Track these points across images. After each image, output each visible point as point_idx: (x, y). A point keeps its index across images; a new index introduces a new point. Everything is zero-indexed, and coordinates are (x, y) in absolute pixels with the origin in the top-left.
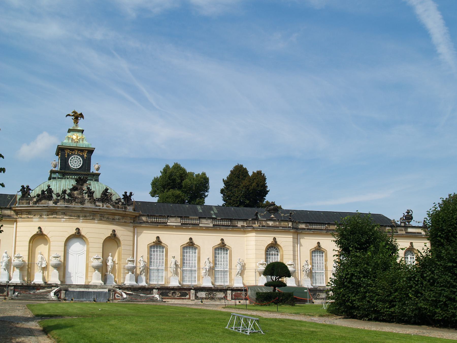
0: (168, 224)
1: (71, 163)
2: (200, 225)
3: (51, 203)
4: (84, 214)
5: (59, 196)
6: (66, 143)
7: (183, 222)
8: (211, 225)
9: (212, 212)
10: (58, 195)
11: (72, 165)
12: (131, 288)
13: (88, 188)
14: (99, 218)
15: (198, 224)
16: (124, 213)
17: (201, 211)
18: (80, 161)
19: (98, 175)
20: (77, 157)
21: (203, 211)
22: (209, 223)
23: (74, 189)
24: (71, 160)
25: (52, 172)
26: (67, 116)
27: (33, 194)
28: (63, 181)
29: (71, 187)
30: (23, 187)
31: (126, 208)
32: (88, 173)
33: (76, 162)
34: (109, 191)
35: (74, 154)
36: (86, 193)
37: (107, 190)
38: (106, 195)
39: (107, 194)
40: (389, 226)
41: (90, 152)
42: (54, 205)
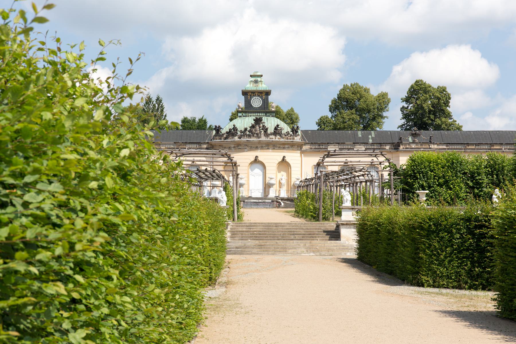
0: (328, 149)
1: (253, 103)
2: (355, 149)
3: (236, 138)
5: (242, 132)
6: (248, 88)
8: (364, 149)
9: (370, 137)
10: (241, 132)
11: (254, 105)
12: (288, 199)
13: (263, 126)
16: (292, 143)
17: (360, 136)
18: (260, 101)
20: (258, 98)
21: (362, 136)
22: (362, 148)
23: (253, 127)
24: (253, 101)
27: (223, 131)
28: (247, 118)
29: (251, 125)
31: (293, 139)
33: (257, 102)
34: (279, 127)
36: (262, 129)
37: (278, 126)
39: (279, 128)
41: (268, 93)
42: (239, 140)
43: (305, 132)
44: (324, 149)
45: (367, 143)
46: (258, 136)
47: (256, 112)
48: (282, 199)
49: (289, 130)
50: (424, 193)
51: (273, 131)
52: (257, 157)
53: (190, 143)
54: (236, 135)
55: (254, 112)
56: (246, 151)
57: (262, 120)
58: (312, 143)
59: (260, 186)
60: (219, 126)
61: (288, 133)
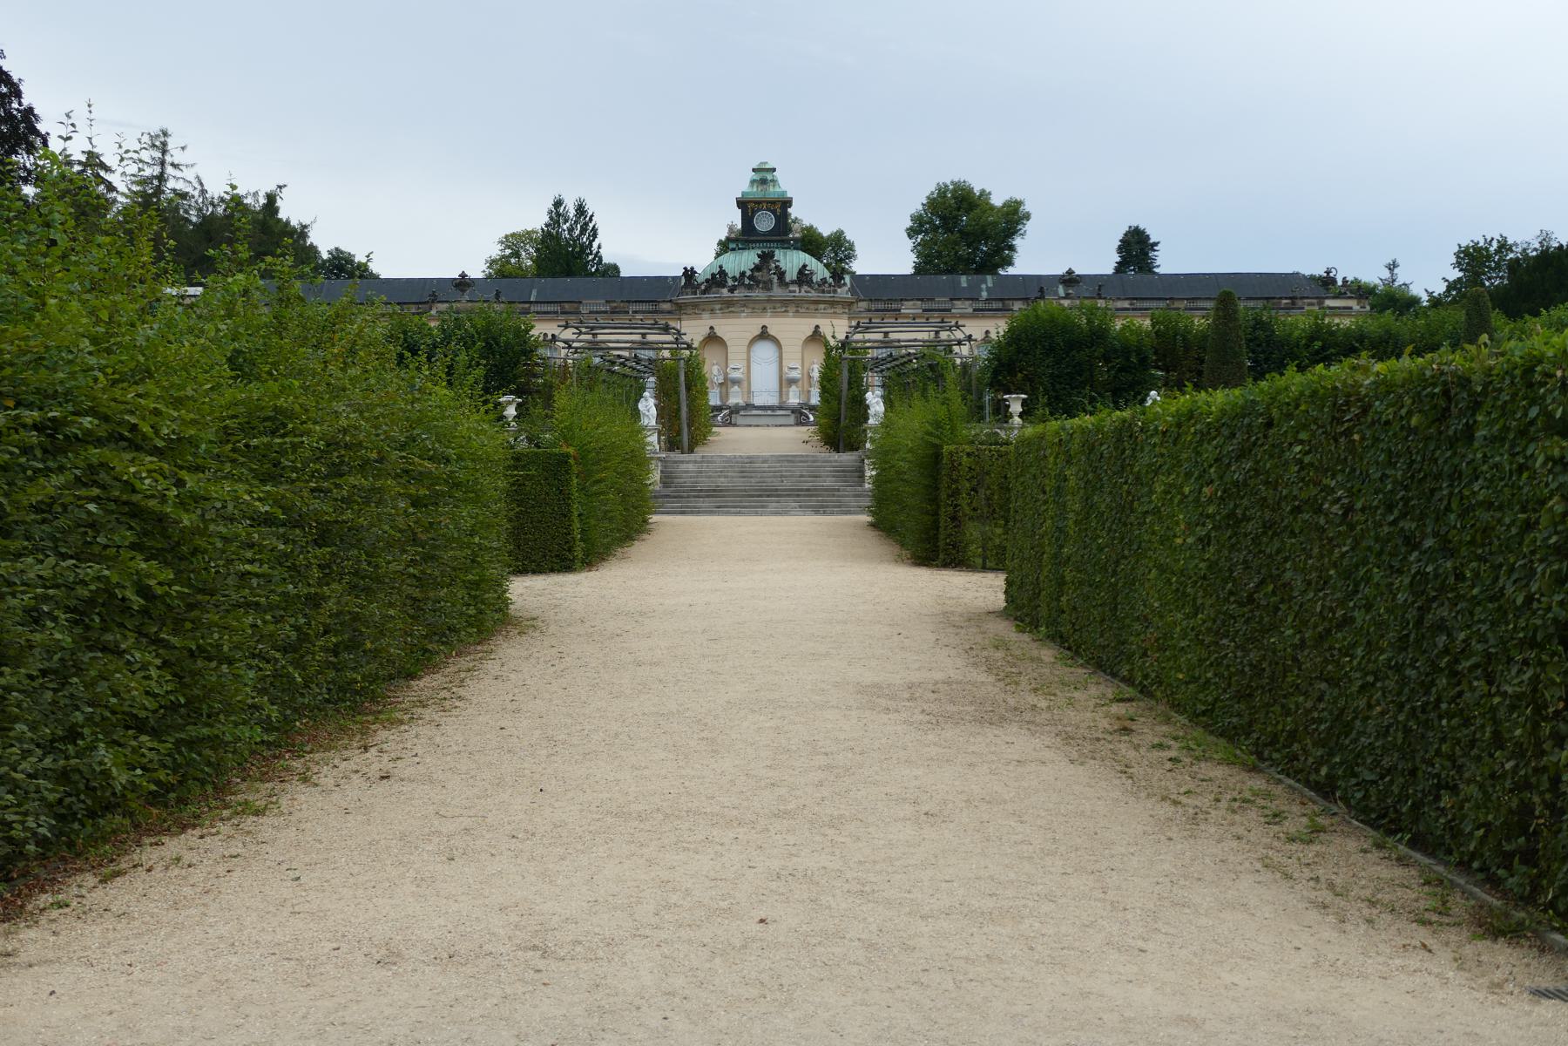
2: (953, 311)
3: (725, 291)
4: (771, 305)
7: (925, 306)
8: (970, 310)
9: (984, 286)
10: (734, 279)
13: (777, 267)
14: (795, 309)
15: (950, 310)
17: (964, 284)
21: (969, 284)
23: (757, 268)
27: (700, 278)
28: (746, 253)
29: (753, 266)
30: (685, 268)
31: (835, 292)
32: (784, 238)
35: (762, 209)
37: (805, 266)
40: (1286, 298)
41: (787, 203)
43: (859, 280)
44: (895, 310)
45: (977, 299)
46: (767, 286)
47: (763, 241)
49: (827, 274)
50: (1018, 398)
51: (795, 278)
52: (764, 327)
53: (636, 302)
54: (724, 286)
55: (759, 241)
56: (745, 317)
57: (773, 256)
58: (871, 300)
59: (773, 384)
60: (692, 268)
61: (824, 281)
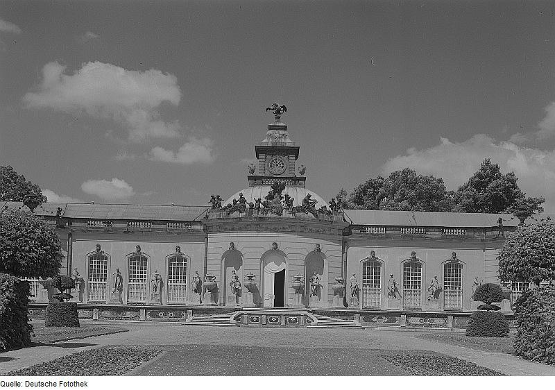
10: (252, 206)
19: (304, 179)
23: (270, 197)
25: (249, 178)
26: (267, 109)
30: (213, 197)
38: (308, 203)
39: (310, 201)
48: (314, 312)
